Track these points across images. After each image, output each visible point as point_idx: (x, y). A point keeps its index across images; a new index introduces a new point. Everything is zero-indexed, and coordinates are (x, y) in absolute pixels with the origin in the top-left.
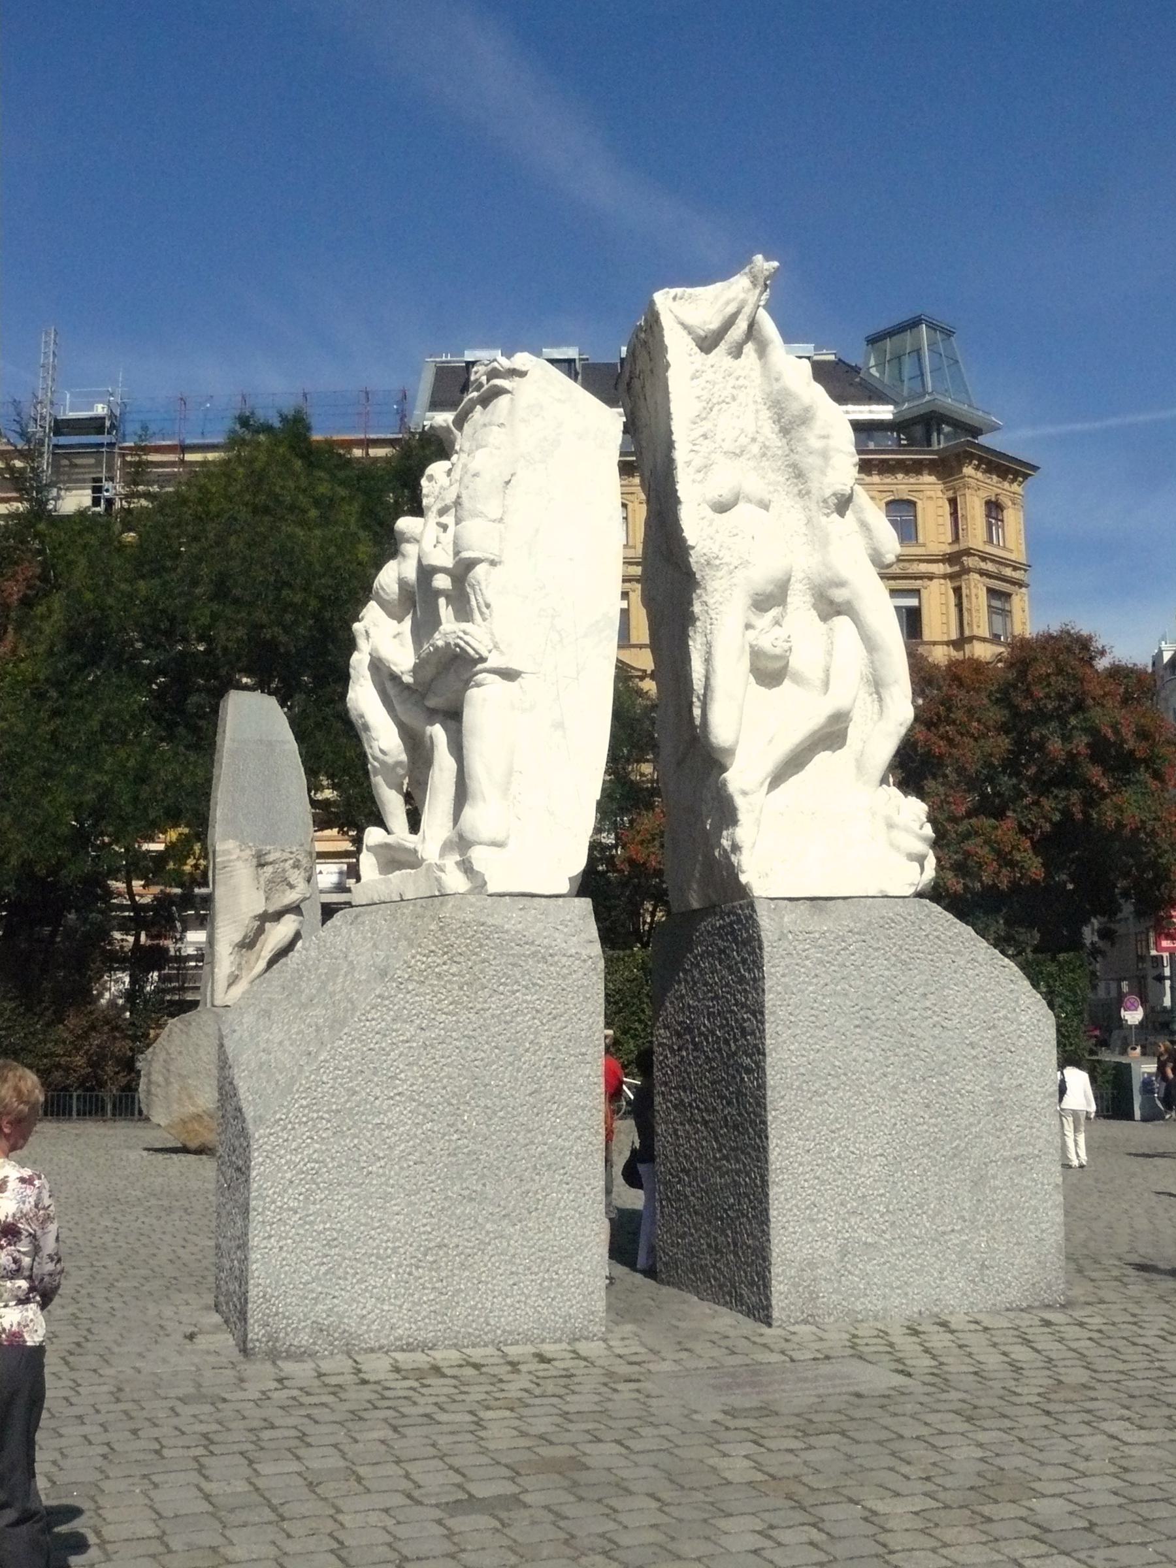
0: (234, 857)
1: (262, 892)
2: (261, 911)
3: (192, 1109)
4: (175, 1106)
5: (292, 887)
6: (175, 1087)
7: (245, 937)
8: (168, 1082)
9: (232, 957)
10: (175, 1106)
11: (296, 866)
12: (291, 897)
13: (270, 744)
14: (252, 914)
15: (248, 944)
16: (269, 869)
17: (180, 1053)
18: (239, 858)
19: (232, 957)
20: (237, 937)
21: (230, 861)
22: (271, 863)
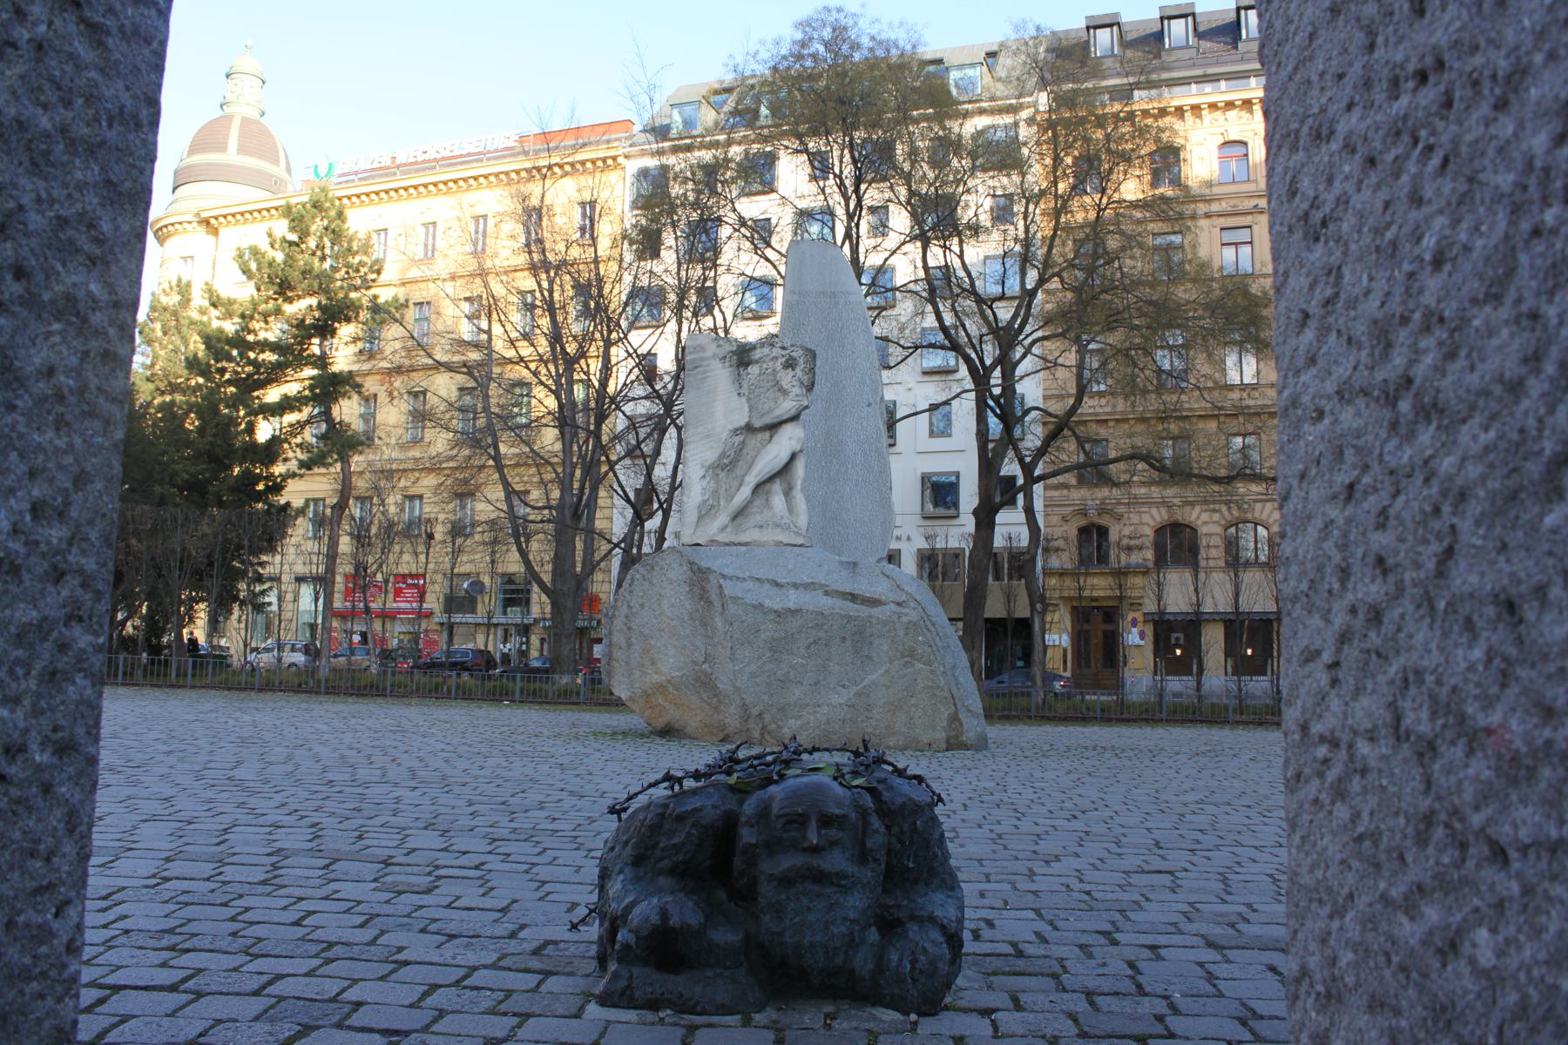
0: (709, 354)
1: (744, 399)
2: (743, 423)
3: (656, 678)
4: (637, 673)
5: (785, 393)
6: (637, 647)
7: (723, 455)
8: (630, 645)
9: (704, 483)
10: (637, 673)
11: (790, 364)
12: (787, 406)
13: (833, 295)
14: (730, 427)
15: (727, 465)
16: (754, 370)
17: (642, 606)
18: (714, 356)
19: (704, 483)
20: (711, 456)
21: (702, 359)
22: (757, 362)
